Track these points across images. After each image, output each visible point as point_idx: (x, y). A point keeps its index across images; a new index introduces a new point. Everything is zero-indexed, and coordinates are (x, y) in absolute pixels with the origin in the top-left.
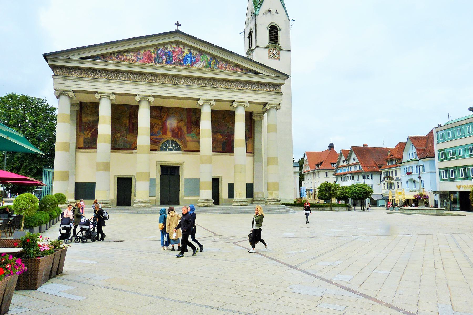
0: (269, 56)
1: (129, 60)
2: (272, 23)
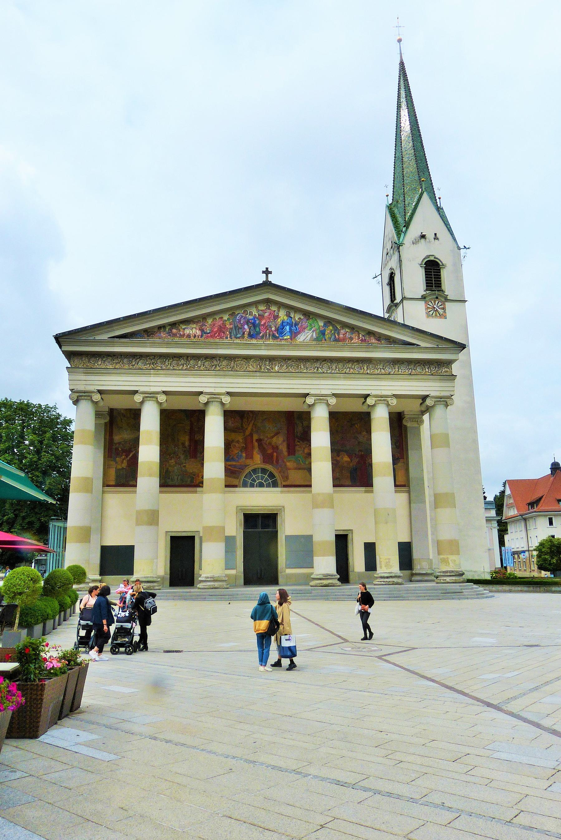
0: (426, 313)
1: (189, 336)
2: (428, 256)
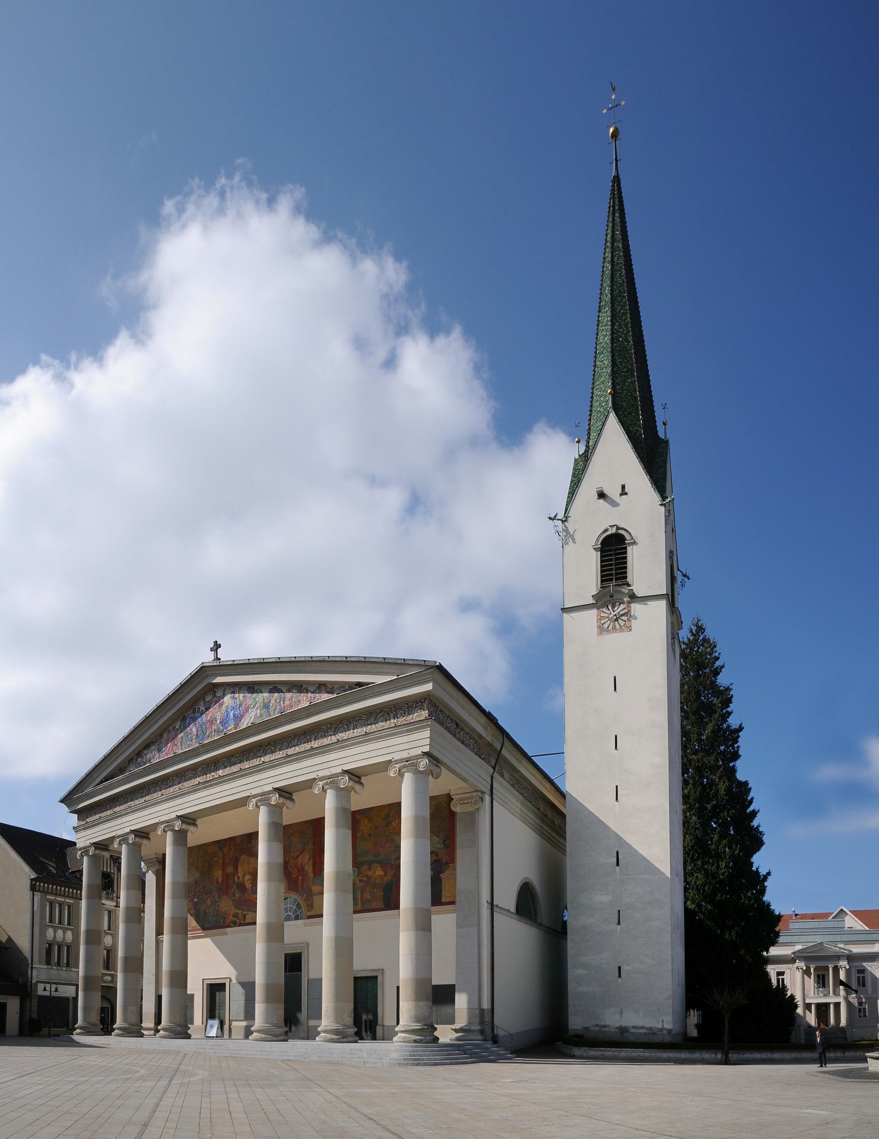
0: (599, 627)
2: (606, 530)
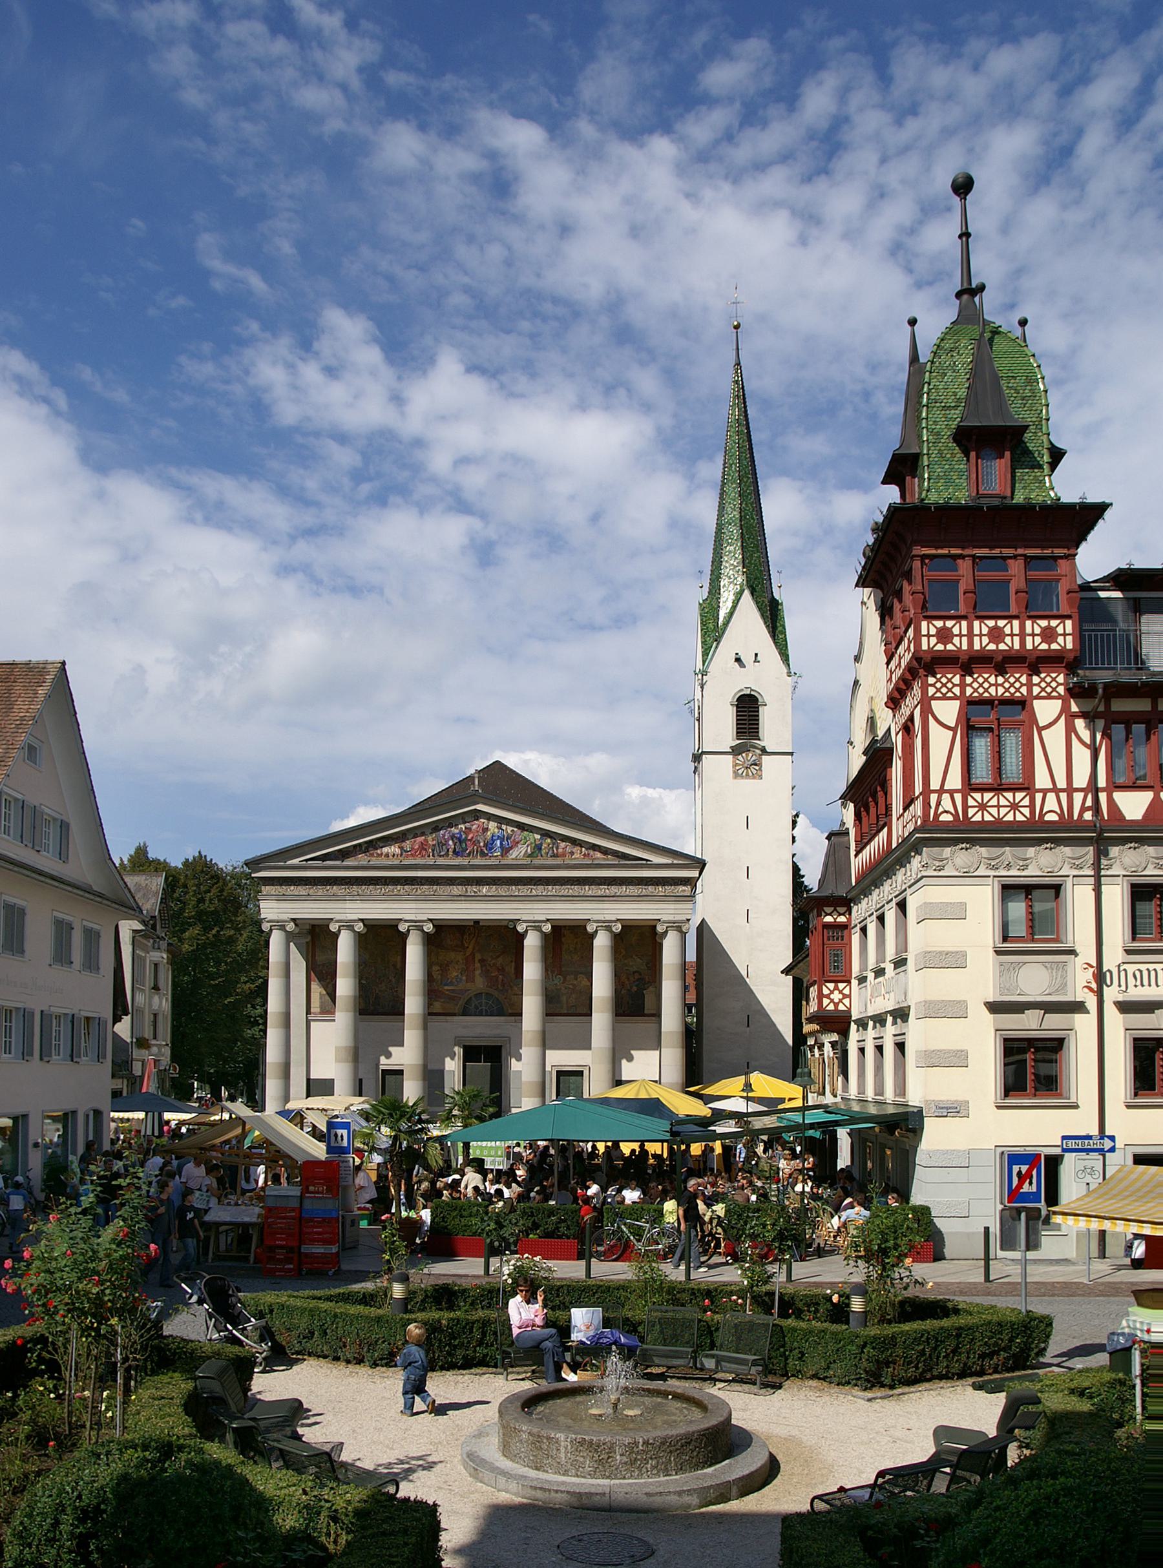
0: (734, 772)
1: (387, 855)
2: (742, 690)
